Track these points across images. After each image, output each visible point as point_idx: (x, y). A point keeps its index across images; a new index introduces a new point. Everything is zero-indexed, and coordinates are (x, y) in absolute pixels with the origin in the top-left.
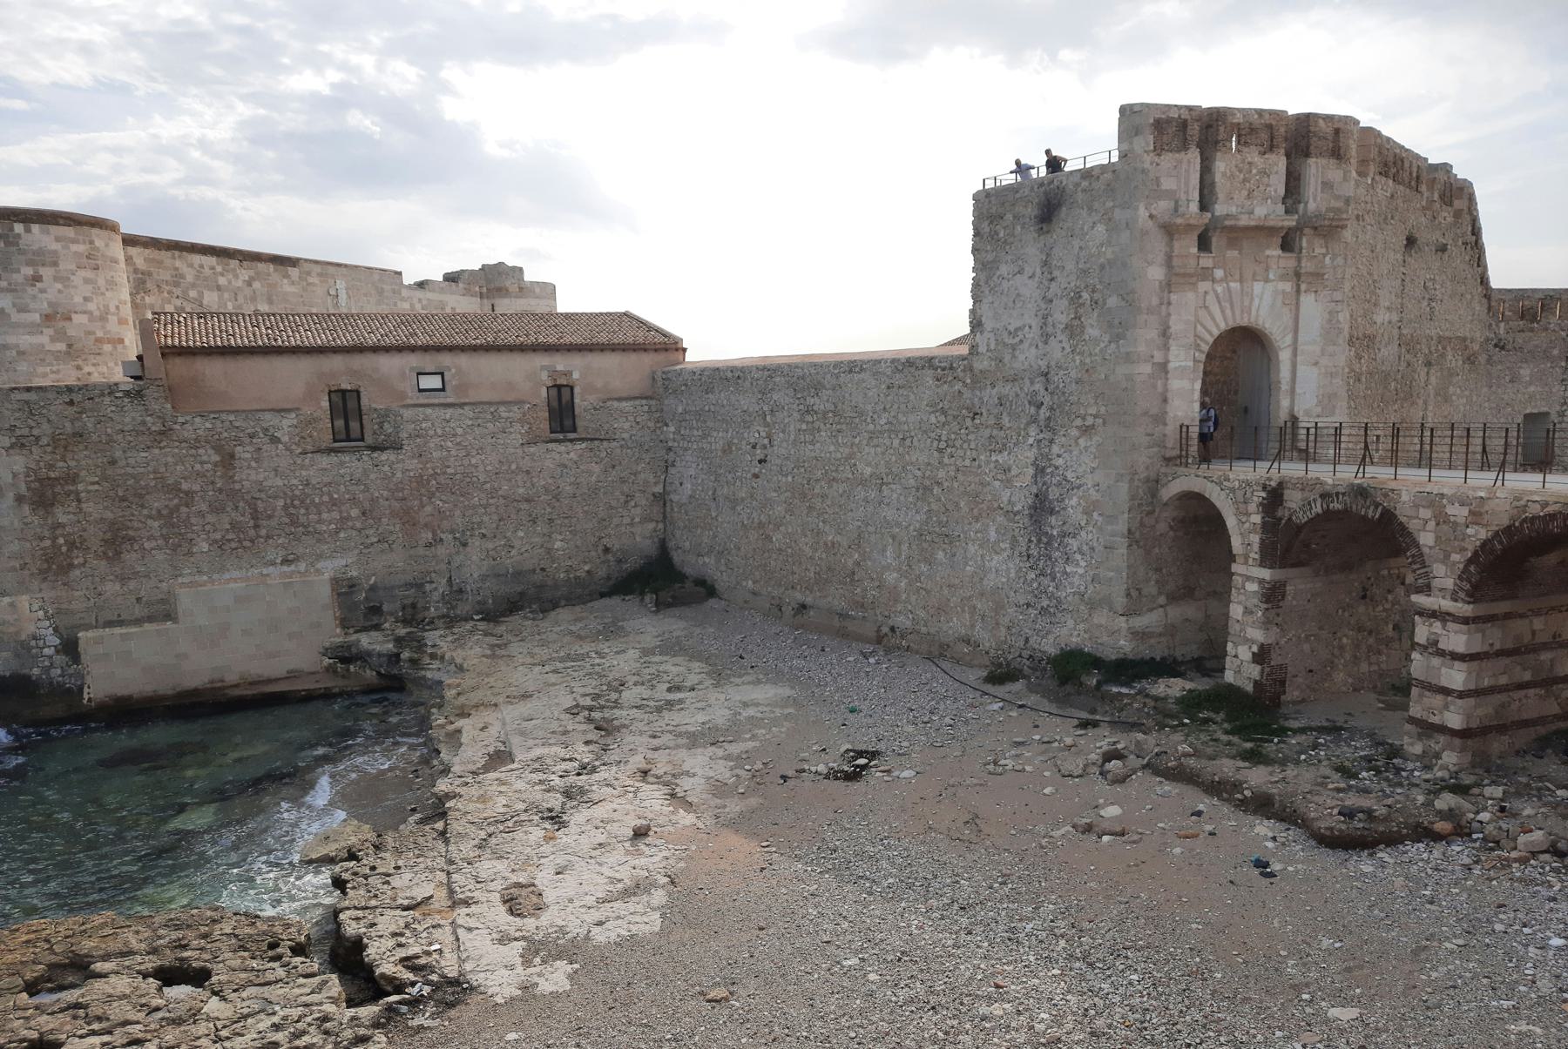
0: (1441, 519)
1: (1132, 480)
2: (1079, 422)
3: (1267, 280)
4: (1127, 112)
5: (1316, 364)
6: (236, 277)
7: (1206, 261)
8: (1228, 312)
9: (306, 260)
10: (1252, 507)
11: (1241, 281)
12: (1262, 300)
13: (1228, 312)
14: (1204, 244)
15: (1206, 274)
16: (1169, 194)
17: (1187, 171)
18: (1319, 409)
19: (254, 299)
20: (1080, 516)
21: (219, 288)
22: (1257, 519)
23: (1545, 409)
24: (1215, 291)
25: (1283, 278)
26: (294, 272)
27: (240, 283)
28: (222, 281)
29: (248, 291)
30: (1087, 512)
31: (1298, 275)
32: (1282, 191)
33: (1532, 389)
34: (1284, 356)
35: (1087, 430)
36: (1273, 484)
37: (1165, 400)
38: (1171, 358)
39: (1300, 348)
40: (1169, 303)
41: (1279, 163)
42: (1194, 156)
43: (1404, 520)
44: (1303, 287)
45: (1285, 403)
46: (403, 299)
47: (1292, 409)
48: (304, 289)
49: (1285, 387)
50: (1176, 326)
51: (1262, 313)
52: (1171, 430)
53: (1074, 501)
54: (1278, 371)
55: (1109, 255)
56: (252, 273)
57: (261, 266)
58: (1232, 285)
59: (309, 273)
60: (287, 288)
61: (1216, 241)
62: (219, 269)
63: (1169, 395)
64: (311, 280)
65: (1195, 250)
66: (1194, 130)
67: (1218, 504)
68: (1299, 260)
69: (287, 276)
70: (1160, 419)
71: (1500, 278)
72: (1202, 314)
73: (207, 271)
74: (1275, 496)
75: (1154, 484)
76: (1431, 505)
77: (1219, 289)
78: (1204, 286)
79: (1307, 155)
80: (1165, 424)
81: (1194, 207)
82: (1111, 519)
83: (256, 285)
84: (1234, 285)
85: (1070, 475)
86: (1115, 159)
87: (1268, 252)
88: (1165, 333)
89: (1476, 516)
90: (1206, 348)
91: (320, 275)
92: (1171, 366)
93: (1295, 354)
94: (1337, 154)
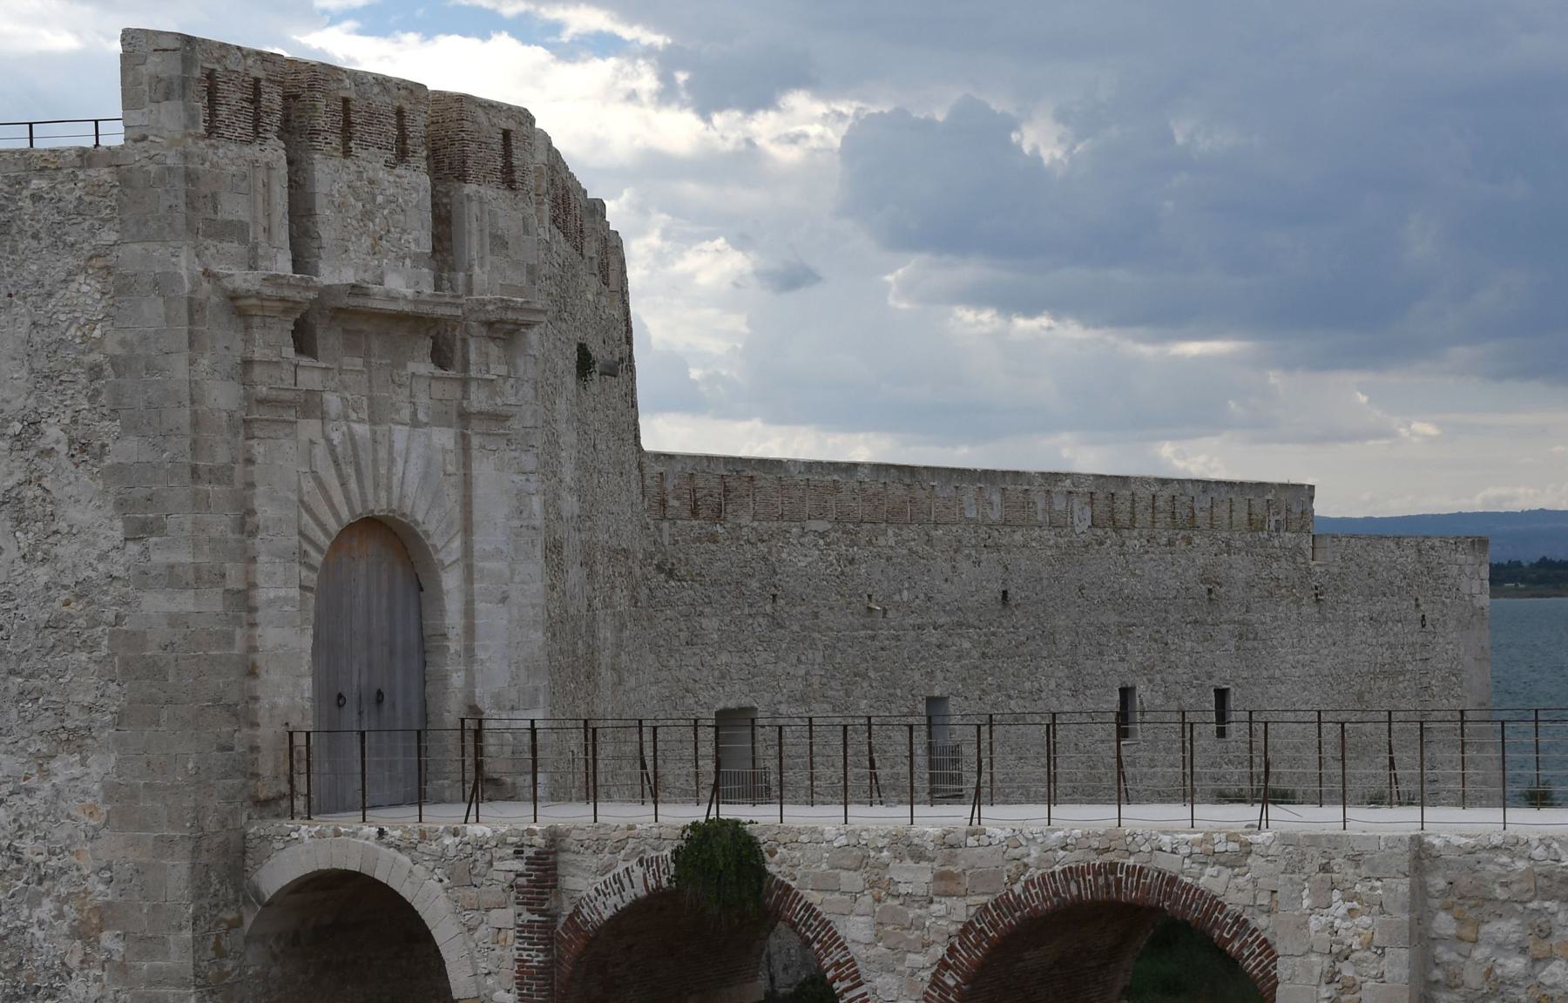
0: (881, 886)
1: (196, 850)
2: (47, 721)
3: (415, 423)
4: (129, 36)
5: (504, 599)
7: (310, 379)
8: (353, 485)
10: (493, 894)
11: (373, 421)
12: (413, 463)
13: (353, 485)
14: (303, 340)
15: (310, 405)
16: (236, 230)
17: (267, 186)
18: (513, 695)
20: (63, 945)
22: (507, 917)
23: (746, 702)
24: (329, 441)
25: (440, 420)
30: (83, 933)
31: (464, 416)
32: (427, 247)
33: (724, 658)
34: (451, 581)
35: (74, 740)
36: (539, 841)
37: (252, 672)
38: (260, 579)
39: (479, 564)
40: (250, 461)
41: (416, 181)
42: (274, 152)
43: (814, 897)
44: (475, 441)
45: (457, 679)
47: (470, 694)
49: (454, 645)
50: (266, 511)
51: (412, 488)
52: (268, 733)
53: (46, 909)
54: (442, 611)
55: (112, 347)
58: (357, 428)
61: (328, 339)
63: (259, 658)
65: (289, 352)
66: (273, 99)
67: (406, 892)
68: (465, 383)
70: (243, 713)
71: (663, 433)
72: (299, 483)
74: (543, 867)
75: (236, 860)
76: (862, 863)
77: (336, 438)
78: (309, 428)
79: (463, 178)
80: (254, 725)
81: (283, 264)
82: (148, 944)
84: (362, 430)
85: (27, 846)
86: (113, 136)
87: (412, 367)
88: (245, 523)
89: (946, 883)
90: (317, 558)
92: (263, 594)
93: (469, 578)
94: (509, 178)
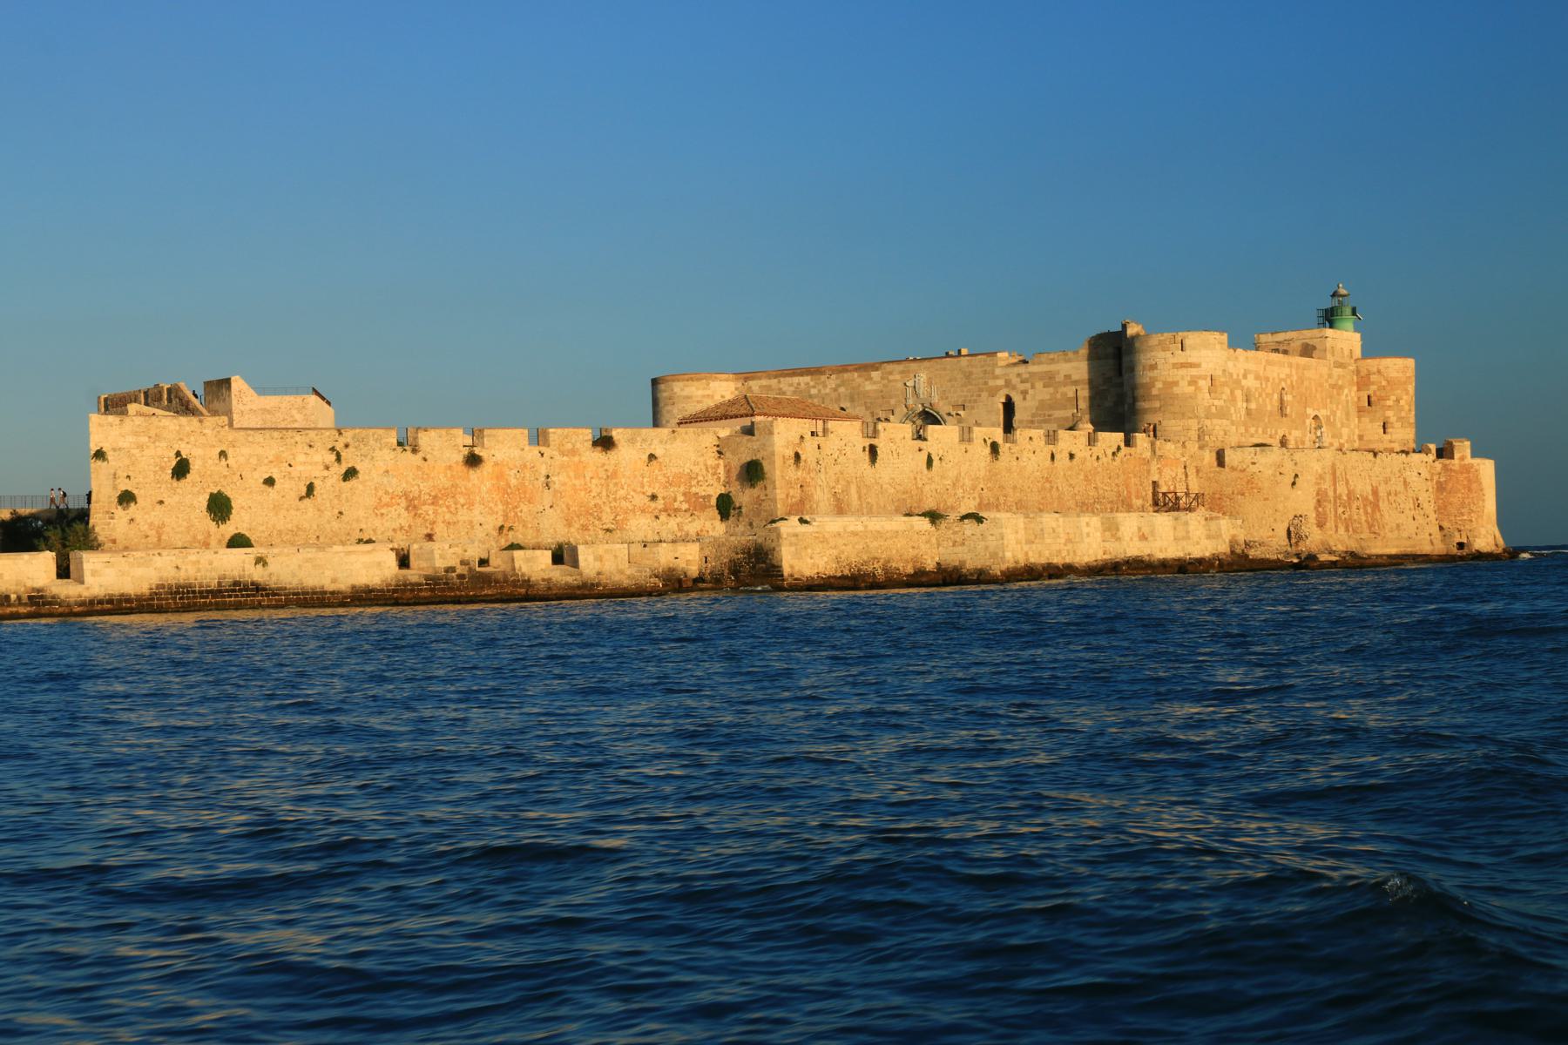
19: (838, 400)
46: (997, 377)
60: (868, 387)
91: (902, 372)
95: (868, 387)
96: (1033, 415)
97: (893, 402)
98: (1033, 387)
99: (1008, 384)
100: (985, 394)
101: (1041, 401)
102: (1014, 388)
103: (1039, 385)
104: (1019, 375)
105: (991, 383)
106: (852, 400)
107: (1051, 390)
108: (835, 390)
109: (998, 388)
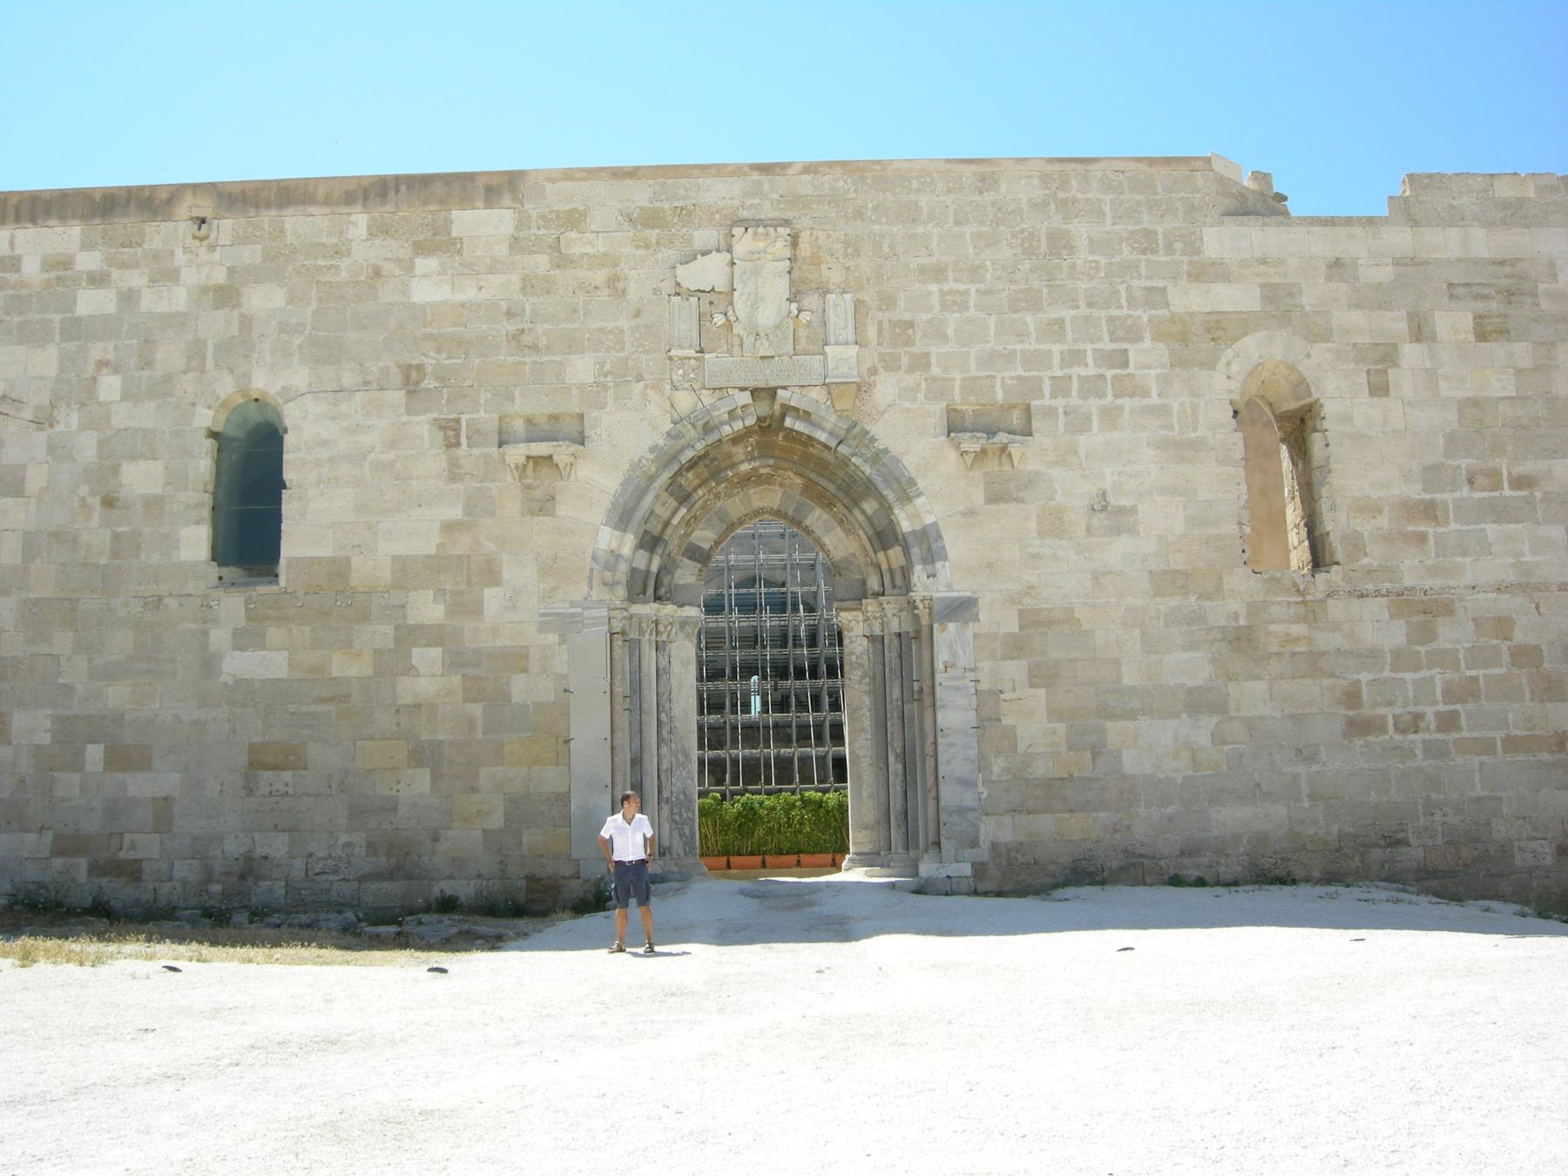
6: (166, 275)
9: (569, 175)
21: (75, 329)
26: (468, 221)
27: (178, 299)
28: (92, 303)
29: (215, 325)
46: (1204, 273)
48: (527, 285)
56: (250, 255)
57: (297, 224)
59: (574, 219)
60: (430, 286)
62: (89, 261)
64: (577, 244)
69: (440, 242)
73: (31, 268)
83: (264, 300)
95: (430, 286)
96: (1432, 475)
97: (582, 369)
98: (1420, 331)
99: (1279, 304)
100: (1147, 357)
101: (1473, 405)
102: (1318, 333)
103: (1453, 322)
104: (1337, 266)
105: (1189, 300)
106: (325, 352)
107: (1522, 353)
108: (225, 296)
109: (1221, 330)
